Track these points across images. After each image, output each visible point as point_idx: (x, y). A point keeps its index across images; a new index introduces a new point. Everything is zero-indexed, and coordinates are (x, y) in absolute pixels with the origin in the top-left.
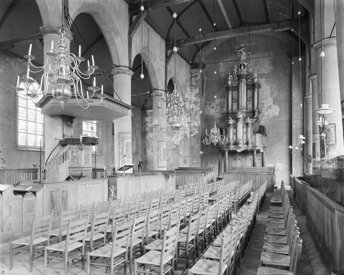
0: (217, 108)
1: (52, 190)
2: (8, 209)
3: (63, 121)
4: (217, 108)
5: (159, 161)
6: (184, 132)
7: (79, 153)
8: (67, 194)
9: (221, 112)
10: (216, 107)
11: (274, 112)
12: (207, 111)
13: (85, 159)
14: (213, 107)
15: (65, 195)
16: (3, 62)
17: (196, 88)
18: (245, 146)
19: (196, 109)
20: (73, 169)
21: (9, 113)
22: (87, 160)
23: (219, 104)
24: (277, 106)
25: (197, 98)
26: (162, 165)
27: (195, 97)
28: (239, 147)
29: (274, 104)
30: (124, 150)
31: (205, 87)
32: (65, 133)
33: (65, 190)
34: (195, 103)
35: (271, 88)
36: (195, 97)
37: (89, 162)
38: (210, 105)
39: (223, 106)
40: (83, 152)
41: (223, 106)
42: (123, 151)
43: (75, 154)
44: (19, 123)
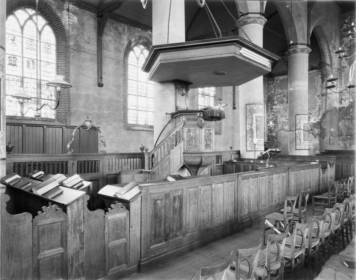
1: (155, 196)
2: (78, 236)
3: (176, 88)
5: (298, 141)
7: (197, 132)
8: (181, 203)
13: (206, 140)
15: (179, 204)
16: (112, 29)
20: (190, 155)
21: (118, 86)
22: (209, 143)
26: (302, 147)
30: (253, 127)
32: (178, 105)
33: (178, 196)
37: (211, 145)
40: (203, 130)
42: (252, 129)
43: (191, 134)
44: (129, 99)
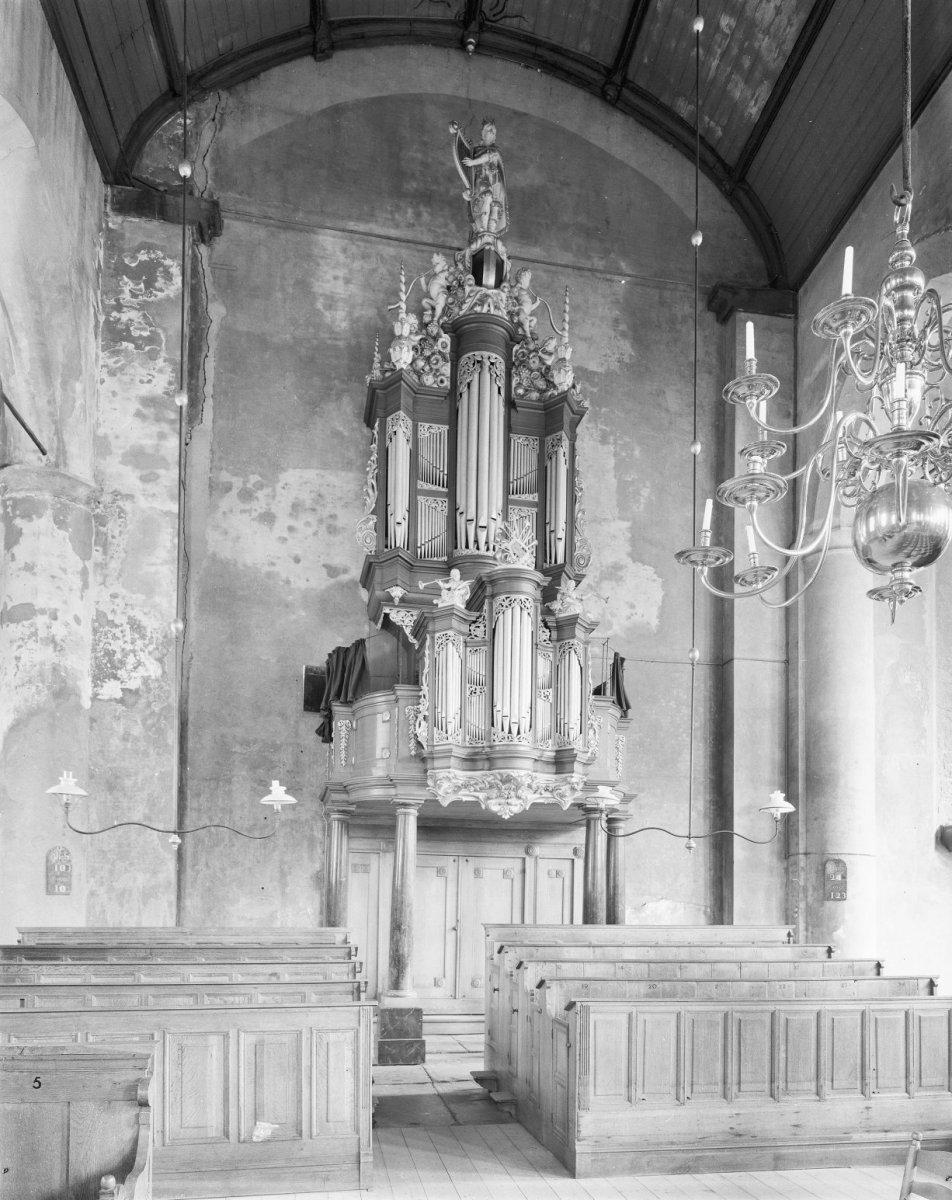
0: (299, 524)
4: (299, 524)
6: (48, 655)
9: (324, 560)
10: (292, 522)
11: (632, 606)
12: (226, 533)
14: (268, 518)
17: (152, 356)
18: (546, 778)
19: (143, 503)
23: (308, 503)
24: (649, 571)
25: (155, 429)
27: (138, 414)
28: (507, 780)
29: (636, 556)
31: (210, 365)
34: (137, 457)
35: (621, 466)
36: (138, 414)
38: (246, 495)
39: (333, 517)
41: (333, 517)
